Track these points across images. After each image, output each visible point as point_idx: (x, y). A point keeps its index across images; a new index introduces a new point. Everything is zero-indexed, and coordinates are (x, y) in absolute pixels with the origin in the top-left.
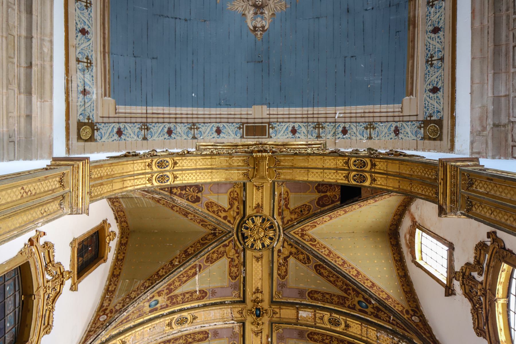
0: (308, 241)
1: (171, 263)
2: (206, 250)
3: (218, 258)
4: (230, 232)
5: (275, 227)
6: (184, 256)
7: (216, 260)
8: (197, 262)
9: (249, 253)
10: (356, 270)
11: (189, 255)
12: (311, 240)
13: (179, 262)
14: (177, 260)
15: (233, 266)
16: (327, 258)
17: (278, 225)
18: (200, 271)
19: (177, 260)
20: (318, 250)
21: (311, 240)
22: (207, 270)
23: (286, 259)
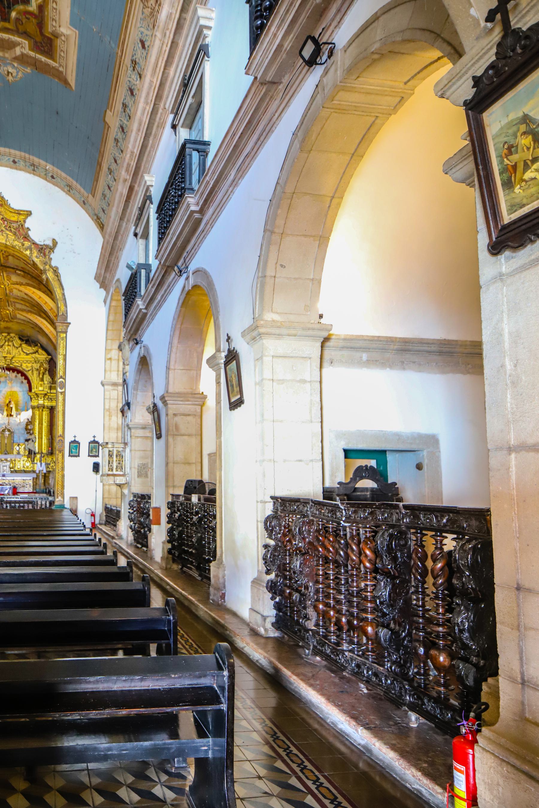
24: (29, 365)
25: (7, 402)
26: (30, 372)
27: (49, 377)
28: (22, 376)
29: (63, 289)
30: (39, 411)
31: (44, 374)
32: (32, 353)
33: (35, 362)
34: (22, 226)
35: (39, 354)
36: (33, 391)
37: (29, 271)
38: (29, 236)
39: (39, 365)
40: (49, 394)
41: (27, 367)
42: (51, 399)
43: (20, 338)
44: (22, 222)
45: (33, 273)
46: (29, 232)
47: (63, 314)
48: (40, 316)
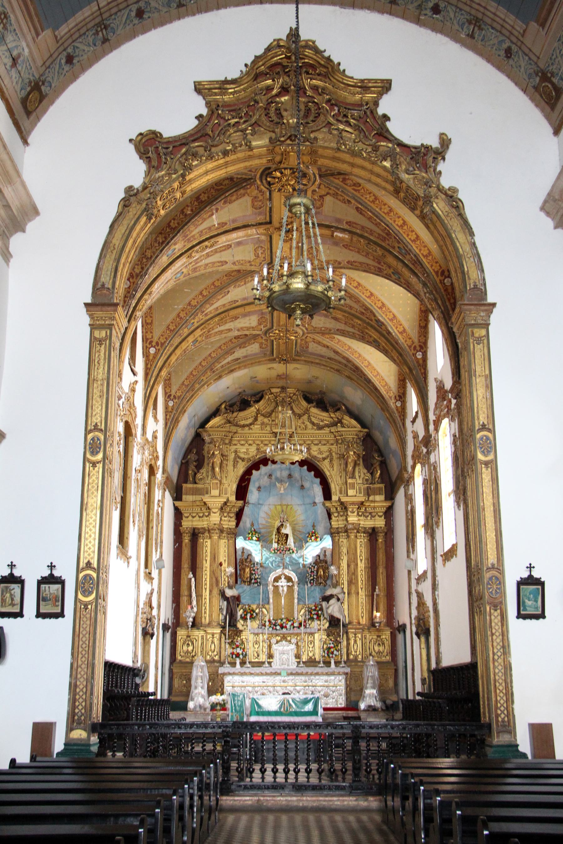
0: (350, 186)
1: (182, 212)
2: (223, 197)
3: (237, 199)
4: (252, 179)
5: (309, 176)
6: (196, 203)
7: (235, 201)
8: (213, 207)
9: (276, 195)
10: (403, 220)
11: (202, 202)
12: (354, 185)
13: (192, 210)
14: (189, 208)
15: (256, 201)
16: (372, 205)
17: (314, 174)
18: (217, 211)
19: (189, 208)
20: (362, 196)
21: (354, 185)
22: (226, 210)
23: (322, 197)
24: (325, 448)
25: (277, 524)
26: (327, 462)
27: (365, 471)
28: (309, 470)
29: (472, 234)
30: (348, 537)
31: (356, 464)
32: (328, 426)
33: (337, 441)
34: (372, 112)
35: (343, 427)
36: (335, 498)
37: (363, 228)
38: (387, 130)
39: (343, 447)
40: (367, 504)
41: (321, 453)
42: (370, 513)
43: (308, 400)
44: (371, 105)
45: (371, 232)
46: (388, 124)
47: (475, 286)
48: (363, 338)
